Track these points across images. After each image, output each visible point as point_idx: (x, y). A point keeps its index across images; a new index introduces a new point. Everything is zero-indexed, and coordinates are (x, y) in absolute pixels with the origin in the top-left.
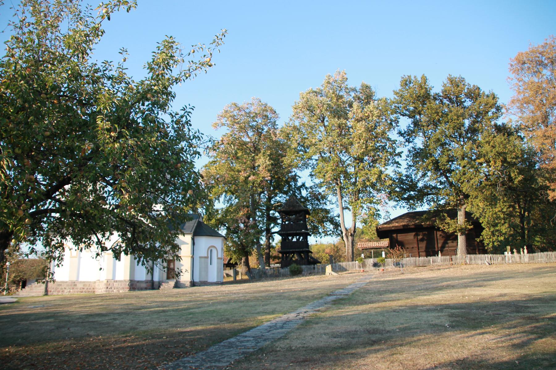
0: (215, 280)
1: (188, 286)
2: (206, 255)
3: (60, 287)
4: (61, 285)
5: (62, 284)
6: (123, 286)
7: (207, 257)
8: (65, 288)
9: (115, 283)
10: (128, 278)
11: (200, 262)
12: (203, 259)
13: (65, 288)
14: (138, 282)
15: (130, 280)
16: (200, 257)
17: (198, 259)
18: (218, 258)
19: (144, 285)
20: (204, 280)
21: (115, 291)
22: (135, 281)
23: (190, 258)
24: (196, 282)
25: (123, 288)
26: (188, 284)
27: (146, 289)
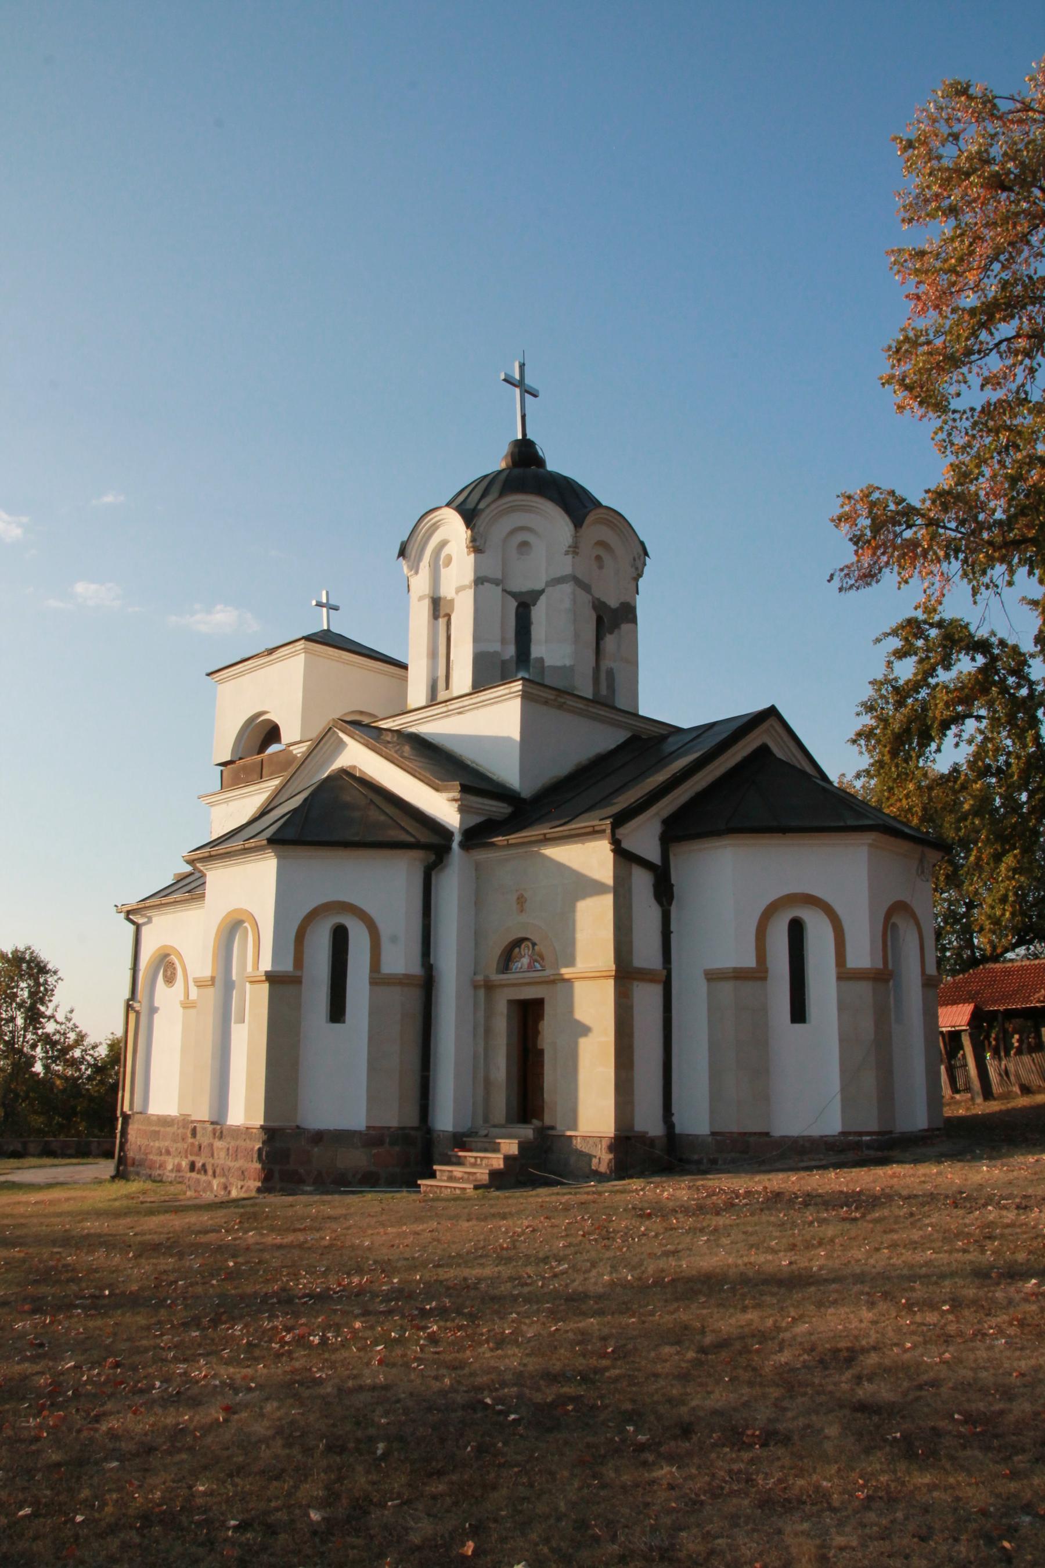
0: (832, 1124)
1: (603, 1168)
2: (750, 961)
3: (157, 1144)
4: (156, 1135)
5: (162, 1129)
6: (240, 1163)
7: (759, 974)
8: (168, 1153)
9: (218, 1144)
10: (259, 1121)
11: (710, 1010)
12: (727, 988)
13: (168, 1153)
14: (319, 1137)
15: (271, 1133)
16: (713, 977)
17: (702, 986)
18: (845, 975)
19: (356, 1159)
20: (734, 1128)
21: (215, 1183)
22: (299, 1131)
23: (610, 985)
24: (692, 1141)
25: (243, 1174)
26: (603, 1159)
27: (369, 1180)
